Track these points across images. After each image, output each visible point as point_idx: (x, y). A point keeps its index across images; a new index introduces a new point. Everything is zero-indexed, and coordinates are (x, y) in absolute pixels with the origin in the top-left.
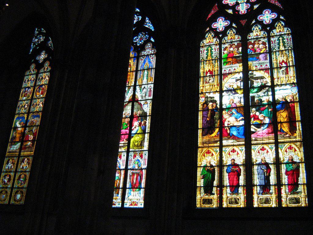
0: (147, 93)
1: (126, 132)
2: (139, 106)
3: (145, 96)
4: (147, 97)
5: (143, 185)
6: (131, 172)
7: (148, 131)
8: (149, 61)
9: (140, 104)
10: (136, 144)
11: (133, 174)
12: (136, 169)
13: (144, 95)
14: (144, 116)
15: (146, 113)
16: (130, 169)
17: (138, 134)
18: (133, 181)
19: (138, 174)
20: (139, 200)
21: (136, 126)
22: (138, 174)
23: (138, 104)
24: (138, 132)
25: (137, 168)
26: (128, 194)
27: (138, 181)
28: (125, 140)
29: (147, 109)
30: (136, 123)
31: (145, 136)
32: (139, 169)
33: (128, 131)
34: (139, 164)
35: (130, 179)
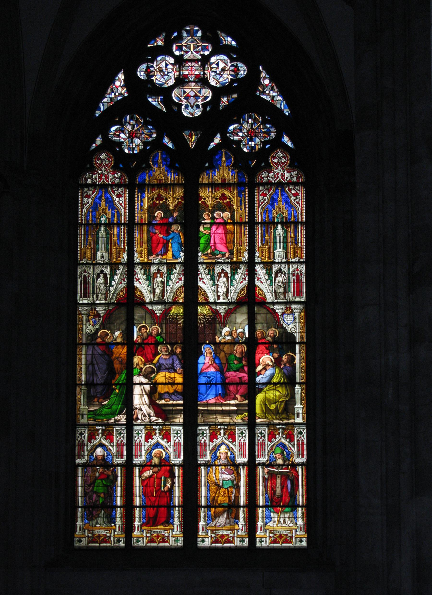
0: (289, 286)
1: (240, 378)
2: (269, 316)
3: (285, 292)
4: (290, 297)
5: (301, 500)
6: (266, 471)
7: (301, 378)
8: (287, 203)
9: (273, 312)
10: (273, 407)
11: (272, 476)
12: (279, 465)
13: (281, 290)
14: (285, 342)
15: (292, 336)
16: (263, 465)
17: (275, 384)
18: (275, 492)
19: (285, 477)
20: (294, 530)
21: (267, 365)
22: (285, 477)
23: (264, 310)
24: (274, 380)
25: (280, 462)
26: (263, 518)
27: (287, 490)
28: (238, 397)
29: (291, 326)
30: (266, 359)
31: (294, 390)
32: (288, 466)
33: (244, 376)
34: (285, 453)
35: (265, 485)
